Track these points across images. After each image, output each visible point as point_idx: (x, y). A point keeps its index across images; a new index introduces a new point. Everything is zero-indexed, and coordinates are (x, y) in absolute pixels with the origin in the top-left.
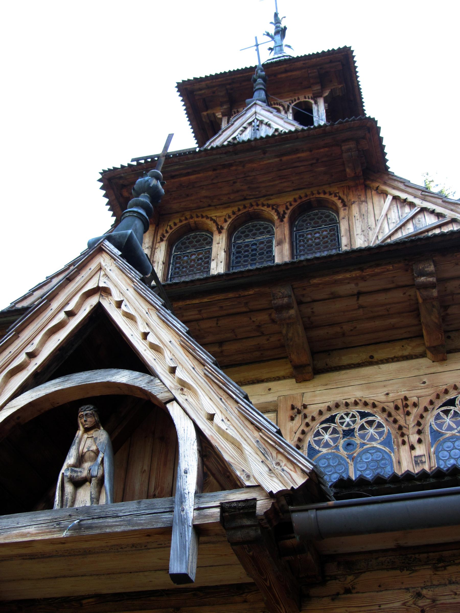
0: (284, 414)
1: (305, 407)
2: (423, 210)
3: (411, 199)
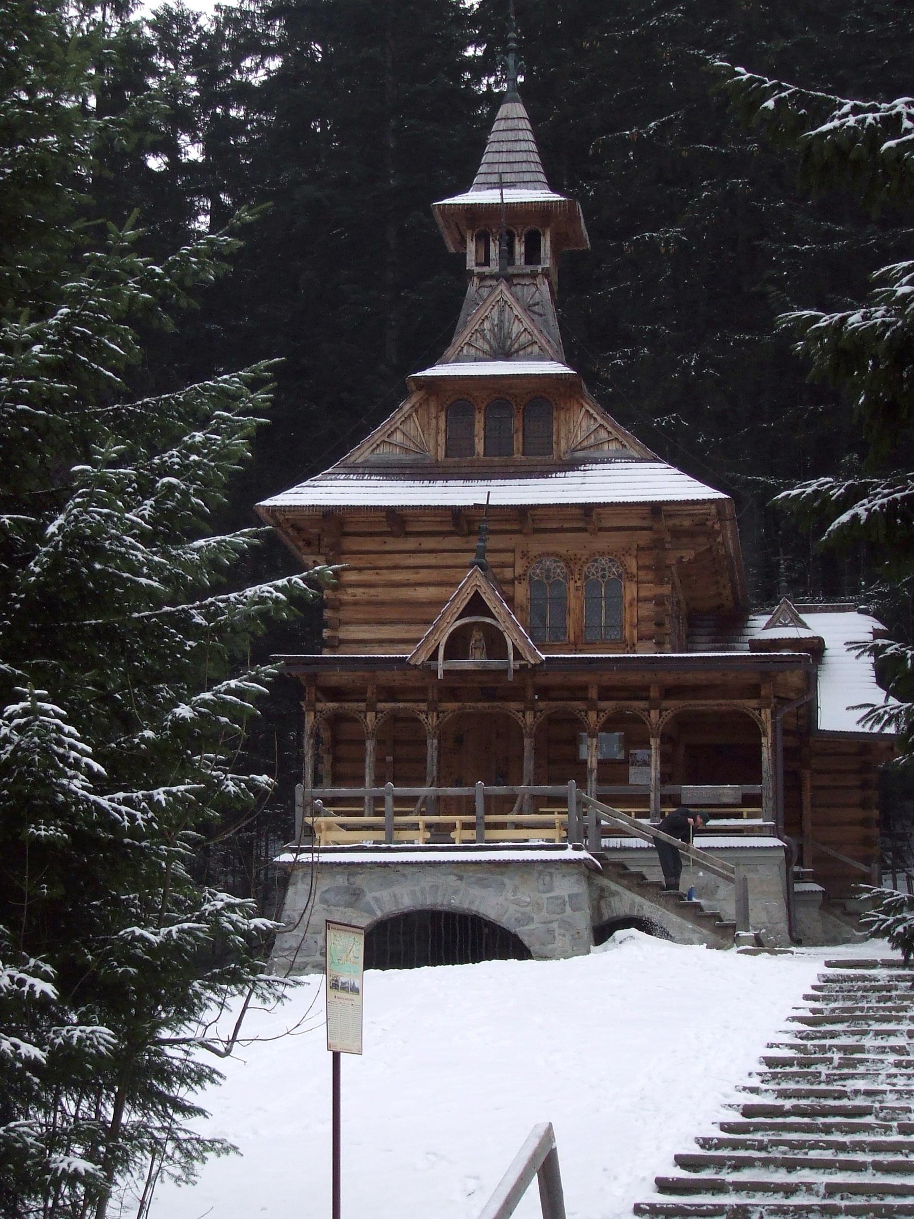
0: (518, 555)
1: (528, 552)
2: (601, 425)
3: (595, 415)
